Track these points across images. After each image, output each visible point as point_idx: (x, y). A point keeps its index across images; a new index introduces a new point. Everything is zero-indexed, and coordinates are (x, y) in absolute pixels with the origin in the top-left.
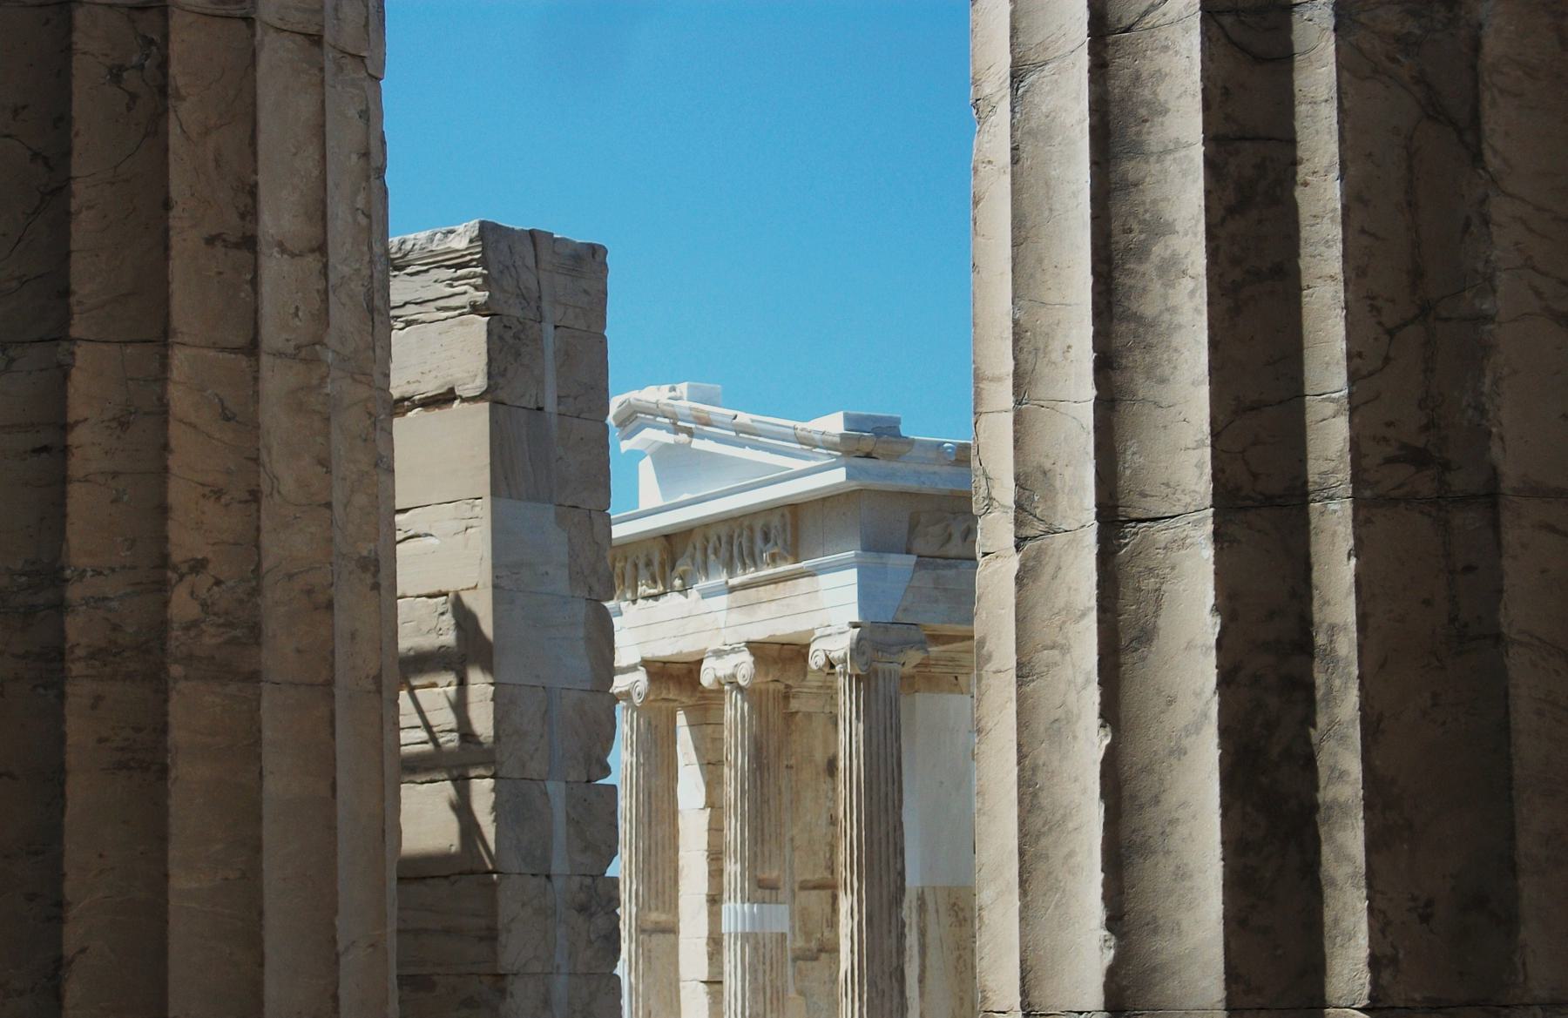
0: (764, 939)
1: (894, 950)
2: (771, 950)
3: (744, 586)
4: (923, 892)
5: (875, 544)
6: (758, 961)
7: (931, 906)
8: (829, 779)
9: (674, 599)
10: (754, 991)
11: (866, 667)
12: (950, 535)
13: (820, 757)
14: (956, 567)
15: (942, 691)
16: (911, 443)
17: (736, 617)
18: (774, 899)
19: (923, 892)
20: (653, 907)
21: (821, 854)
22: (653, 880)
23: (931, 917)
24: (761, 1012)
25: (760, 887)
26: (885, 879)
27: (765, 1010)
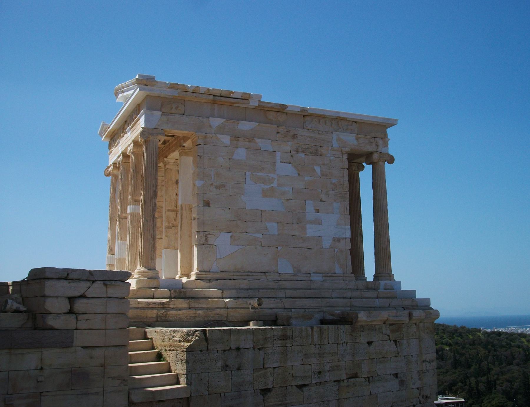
0: (135, 214)
1: (152, 210)
2: (137, 217)
3: (132, 127)
4: (182, 205)
5: (151, 108)
6: (134, 220)
7: (184, 209)
8: (176, 185)
9: (126, 135)
10: (133, 227)
11: (146, 139)
12: (172, 108)
13: (174, 180)
14: (174, 116)
15: (189, 156)
16: (157, 82)
17: (132, 135)
18: (138, 204)
19: (182, 205)
20: (123, 212)
21: (173, 203)
22: (124, 206)
23: (184, 211)
24: (134, 232)
25: (135, 201)
26: (149, 192)
27: (135, 232)
